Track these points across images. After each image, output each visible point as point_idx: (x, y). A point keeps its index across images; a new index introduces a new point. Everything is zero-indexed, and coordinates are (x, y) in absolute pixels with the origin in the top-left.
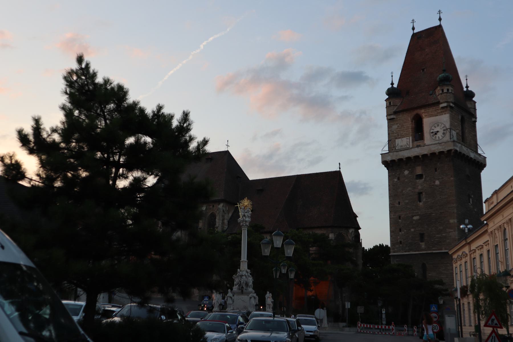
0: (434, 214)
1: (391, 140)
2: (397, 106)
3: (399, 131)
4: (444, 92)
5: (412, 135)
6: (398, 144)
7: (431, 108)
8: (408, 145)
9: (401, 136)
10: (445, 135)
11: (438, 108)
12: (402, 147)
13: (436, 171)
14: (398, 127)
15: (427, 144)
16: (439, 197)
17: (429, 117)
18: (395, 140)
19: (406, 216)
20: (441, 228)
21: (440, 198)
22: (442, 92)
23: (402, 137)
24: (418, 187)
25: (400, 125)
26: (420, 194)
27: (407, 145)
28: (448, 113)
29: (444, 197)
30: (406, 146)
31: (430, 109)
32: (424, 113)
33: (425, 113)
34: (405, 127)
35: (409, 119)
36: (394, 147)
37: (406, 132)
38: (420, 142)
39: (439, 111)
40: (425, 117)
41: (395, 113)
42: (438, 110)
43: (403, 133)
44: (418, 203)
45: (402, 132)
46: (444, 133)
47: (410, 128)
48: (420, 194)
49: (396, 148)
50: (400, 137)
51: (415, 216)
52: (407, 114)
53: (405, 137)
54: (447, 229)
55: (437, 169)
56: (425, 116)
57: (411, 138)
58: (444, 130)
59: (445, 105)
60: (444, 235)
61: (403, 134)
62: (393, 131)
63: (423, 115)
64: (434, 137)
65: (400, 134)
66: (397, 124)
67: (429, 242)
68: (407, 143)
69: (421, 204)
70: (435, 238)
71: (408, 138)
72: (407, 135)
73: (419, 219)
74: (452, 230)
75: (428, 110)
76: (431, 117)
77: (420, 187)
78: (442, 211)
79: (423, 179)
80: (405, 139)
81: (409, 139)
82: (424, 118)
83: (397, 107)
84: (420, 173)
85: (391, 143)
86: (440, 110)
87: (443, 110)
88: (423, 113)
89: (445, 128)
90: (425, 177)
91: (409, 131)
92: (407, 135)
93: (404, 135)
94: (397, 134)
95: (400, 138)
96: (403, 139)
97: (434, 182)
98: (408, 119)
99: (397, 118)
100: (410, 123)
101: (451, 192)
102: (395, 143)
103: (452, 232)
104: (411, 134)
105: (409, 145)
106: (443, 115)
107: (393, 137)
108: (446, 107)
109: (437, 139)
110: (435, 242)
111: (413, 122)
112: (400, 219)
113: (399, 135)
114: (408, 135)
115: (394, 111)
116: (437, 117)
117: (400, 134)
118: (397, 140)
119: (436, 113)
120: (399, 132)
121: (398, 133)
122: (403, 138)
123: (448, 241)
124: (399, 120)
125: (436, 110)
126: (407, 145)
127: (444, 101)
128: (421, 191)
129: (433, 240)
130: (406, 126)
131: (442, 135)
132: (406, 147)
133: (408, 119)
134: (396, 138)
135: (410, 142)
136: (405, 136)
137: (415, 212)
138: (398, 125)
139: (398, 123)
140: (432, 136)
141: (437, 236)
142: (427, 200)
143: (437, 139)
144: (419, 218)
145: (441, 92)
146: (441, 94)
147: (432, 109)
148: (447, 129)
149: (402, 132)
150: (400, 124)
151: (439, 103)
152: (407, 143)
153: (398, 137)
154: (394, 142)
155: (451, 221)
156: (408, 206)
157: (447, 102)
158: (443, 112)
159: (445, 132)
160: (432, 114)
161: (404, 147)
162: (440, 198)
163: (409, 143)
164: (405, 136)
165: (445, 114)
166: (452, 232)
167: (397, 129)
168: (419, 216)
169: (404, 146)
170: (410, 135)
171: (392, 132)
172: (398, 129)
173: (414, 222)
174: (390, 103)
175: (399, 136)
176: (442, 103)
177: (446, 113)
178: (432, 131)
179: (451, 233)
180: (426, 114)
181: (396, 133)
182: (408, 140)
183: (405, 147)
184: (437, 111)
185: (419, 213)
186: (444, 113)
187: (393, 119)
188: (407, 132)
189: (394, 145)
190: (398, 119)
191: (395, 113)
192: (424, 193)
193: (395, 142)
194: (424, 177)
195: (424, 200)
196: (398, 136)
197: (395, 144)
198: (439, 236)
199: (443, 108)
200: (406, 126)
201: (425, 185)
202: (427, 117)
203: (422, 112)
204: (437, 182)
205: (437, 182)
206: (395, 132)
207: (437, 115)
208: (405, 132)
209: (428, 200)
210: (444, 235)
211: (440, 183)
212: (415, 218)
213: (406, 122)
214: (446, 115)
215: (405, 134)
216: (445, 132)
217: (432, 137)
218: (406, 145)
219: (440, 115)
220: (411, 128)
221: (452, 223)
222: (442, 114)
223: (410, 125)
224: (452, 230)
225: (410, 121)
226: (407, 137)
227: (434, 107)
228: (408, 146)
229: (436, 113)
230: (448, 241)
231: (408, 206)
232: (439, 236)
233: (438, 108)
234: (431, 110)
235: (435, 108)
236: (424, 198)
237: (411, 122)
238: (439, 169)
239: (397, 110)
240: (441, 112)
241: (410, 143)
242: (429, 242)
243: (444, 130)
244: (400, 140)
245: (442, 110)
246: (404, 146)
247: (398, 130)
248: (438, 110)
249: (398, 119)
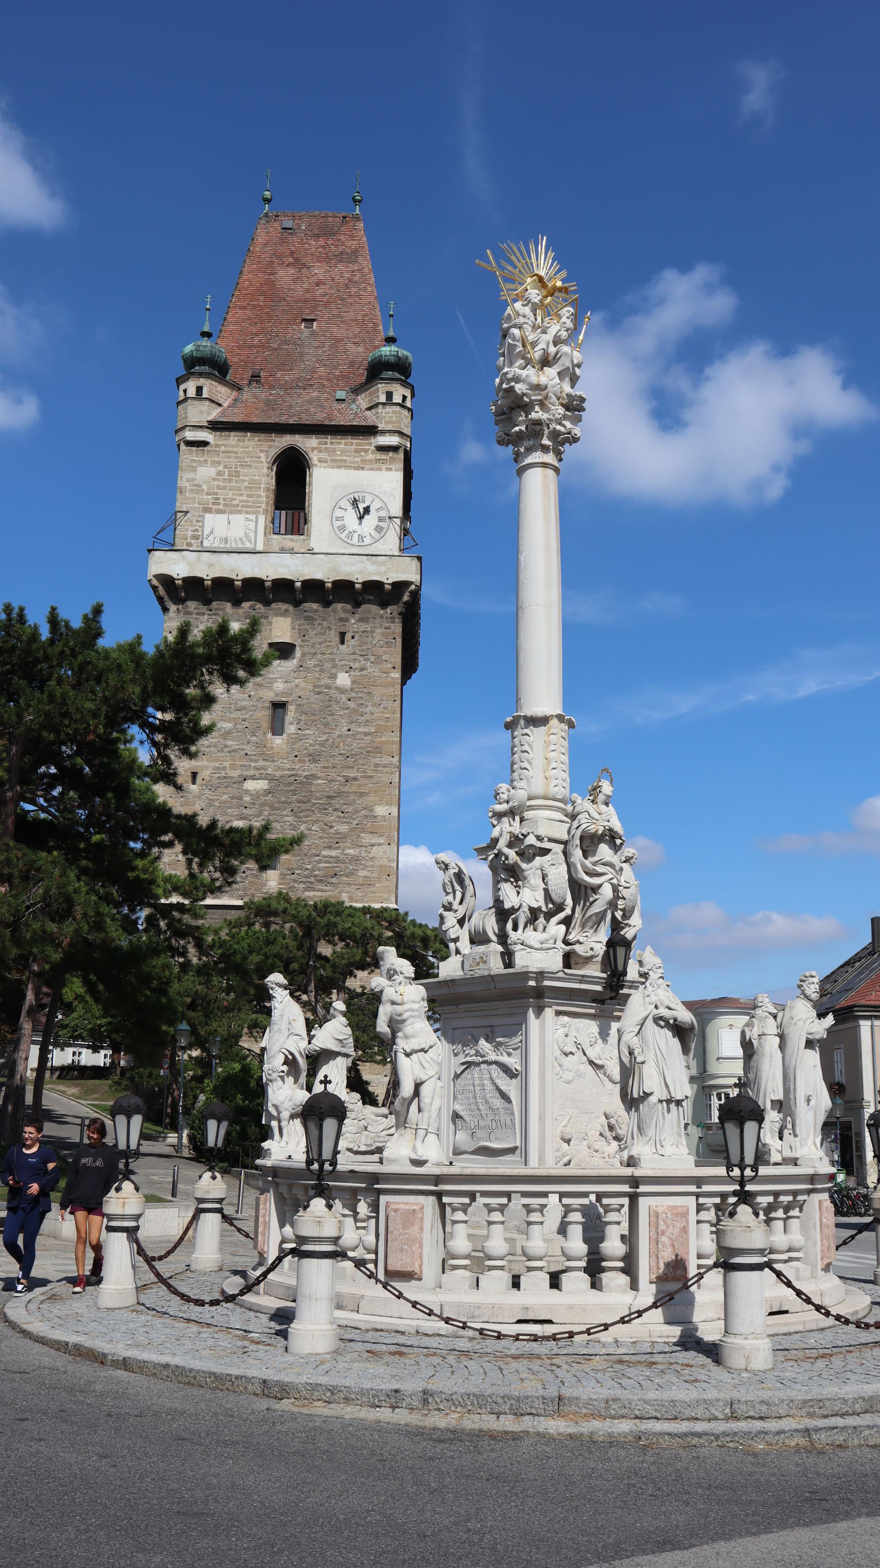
0: (322, 779)
1: (187, 512)
2: (220, 405)
3: (219, 487)
4: (394, 401)
5: (266, 512)
6: (212, 532)
7: (343, 441)
8: (250, 541)
9: (225, 505)
10: (383, 533)
11: (367, 447)
12: (226, 543)
13: (342, 642)
14: (219, 473)
15: (315, 551)
16: (346, 728)
17: (333, 468)
18: (203, 517)
19: (217, 775)
20: (344, 828)
21: (349, 730)
22: (387, 399)
23: (229, 509)
24: (275, 685)
25: (226, 470)
26: (279, 706)
27: (244, 539)
28: (396, 470)
29: (360, 730)
30: (243, 543)
31: (341, 443)
32: (315, 452)
33: (320, 451)
34: (243, 481)
35: (263, 459)
36: (195, 537)
37: (245, 498)
38: (292, 540)
39: (371, 457)
40: (318, 464)
41: (215, 426)
42: (366, 451)
43: (232, 499)
44: (269, 735)
45: (230, 493)
46: (379, 529)
47: (262, 486)
48: (279, 706)
49: (202, 542)
50: (221, 507)
51: (253, 778)
52: (256, 439)
53: (240, 512)
54: (363, 835)
55: (348, 637)
56: (320, 461)
57: (262, 519)
58: (381, 519)
59: (393, 440)
60: (351, 851)
61: (234, 502)
62: (196, 482)
63: (314, 457)
64: (343, 536)
65: (224, 499)
66: (215, 463)
67: (296, 872)
68: (246, 535)
69: (278, 740)
70: (317, 858)
71: (253, 517)
72: (249, 507)
73: (268, 792)
74: (381, 841)
75: (331, 443)
76: (339, 467)
77: (279, 686)
78: (352, 775)
79: (295, 661)
80: (238, 520)
81: (257, 522)
82: (316, 465)
83: (220, 409)
84: (287, 639)
85: (186, 521)
86: (373, 453)
87: (384, 457)
88: (313, 449)
89: (383, 514)
90: (304, 655)
91: (259, 496)
92: (249, 507)
93: (237, 505)
94: (215, 499)
95: (219, 512)
96: (231, 516)
97: (333, 677)
98: (259, 457)
99: (217, 446)
100: (265, 470)
101: (387, 716)
102: (200, 524)
103: (379, 845)
104: (264, 506)
105: (253, 541)
106: (380, 472)
107: (197, 505)
108: (395, 449)
109: (355, 540)
110: (317, 873)
111: (272, 470)
112: (194, 783)
113: (221, 501)
114: (251, 509)
115: (209, 419)
116: (360, 472)
117: (224, 499)
118: (208, 517)
119: (357, 459)
120: (219, 491)
121: (216, 494)
122: (231, 513)
123: (362, 873)
124: (223, 452)
125: (356, 451)
126: (244, 539)
127: (390, 427)
128: (284, 699)
129: (308, 867)
130: (246, 478)
131: (374, 533)
132: (240, 545)
133: (259, 457)
134: (208, 510)
135: (256, 532)
136: (240, 508)
137: (253, 764)
138: (221, 468)
139: (219, 463)
140: (338, 527)
141: (324, 853)
142: (299, 732)
143: (355, 540)
144: (266, 788)
145: (383, 398)
146: (383, 404)
147: (346, 444)
148: (390, 518)
149: (233, 494)
150: (225, 467)
151: (371, 431)
152: (246, 535)
153: (216, 507)
154: (198, 521)
155: (381, 810)
156: (230, 743)
157: (401, 433)
158: (383, 461)
159: (382, 524)
160: (346, 460)
161: (234, 545)
162: (349, 730)
163: (252, 535)
164: (240, 508)
165: (390, 469)
166: (379, 845)
167: (214, 479)
168: (266, 782)
169: (235, 539)
170: (261, 509)
171: (196, 485)
172: (218, 480)
173: (247, 798)
174: (199, 390)
175: (219, 504)
176: (383, 432)
177: (393, 467)
178: (338, 513)
179: (375, 848)
180: (324, 456)
181: (207, 494)
182: (252, 525)
183: (236, 544)
184: (363, 454)
185: (270, 771)
186: (384, 467)
187: (205, 444)
188: (251, 496)
189: (197, 530)
190: (223, 448)
191: (215, 426)
192: (291, 708)
193: (203, 521)
194: (298, 653)
195: (291, 729)
196: (214, 504)
197: (203, 527)
198: (334, 853)
199: (382, 449)
200: (246, 478)
201: (297, 681)
202: (323, 465)
203: (308, 444)
204: (343, 679)
205: (343, 679)
206: (205, 487)
207: (363, 468)
208: (241, 495)
209: (307, 732)
210: (351, 851)
211: (353, 682)
212: (250, 785)
213: (250, 466)
214: (389, 472)
215: (241, 501)
216: (382, 524)
217: (338, 532)
218: (241, 539)
219: (373, 469)
220: (268, 490)
221: (384, 817)
222: (380, 469)
223: (264, 479)
224: (381, 841)
225: (265, 465)
226: (247, 513)
227: (355, 441)
228: (249, 546)
229: (357, 459)
230: (362, 873)
231: (230, 743)
232: (334, 853)
233: (367, 447)
234: (343, 445)
235: (357, 444)
236: (292, 723)
237: (268, 468)
238: (353, 637)
239: (221, 420)
240: (378, 461)
241: (256, 537)
242: (296, 872)
243: (381, 519)
244: (223, 518)
245: (379, 455)
246: (235, 539)
247: (217, 483)
248: (366, 451)
249: (223, 448)
